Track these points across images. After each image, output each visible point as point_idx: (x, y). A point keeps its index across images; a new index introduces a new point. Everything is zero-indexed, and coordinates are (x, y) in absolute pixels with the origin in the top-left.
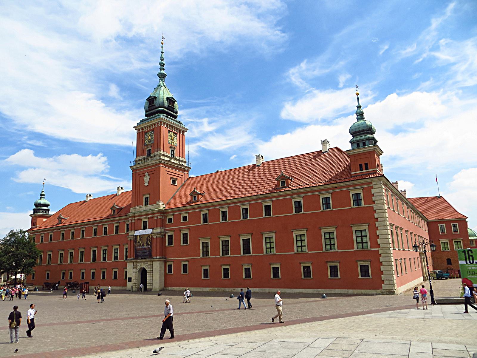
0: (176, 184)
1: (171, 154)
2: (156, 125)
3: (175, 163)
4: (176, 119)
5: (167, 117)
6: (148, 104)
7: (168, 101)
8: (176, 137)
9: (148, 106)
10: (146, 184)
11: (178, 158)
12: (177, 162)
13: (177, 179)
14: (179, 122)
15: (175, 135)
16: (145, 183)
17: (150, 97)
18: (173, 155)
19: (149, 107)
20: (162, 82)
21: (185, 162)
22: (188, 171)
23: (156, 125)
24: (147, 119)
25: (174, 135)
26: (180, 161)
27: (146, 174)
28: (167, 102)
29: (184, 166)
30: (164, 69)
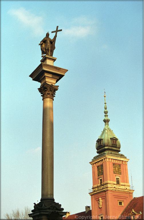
0: (123, 205)
1: (117, 181)
4: (119, 153)
5: (111, 153)
7: (111, 141)
11: (123, 184)
12: (123, 187)
13: (123, 201)
14: (122, 155)
17: (99, 139)
18: (118, 183)
20: (107, 125)
21: (129, 186)
24: (97, 156)
26: (124, 185)
28: (110, 142)
30: (107, 116)
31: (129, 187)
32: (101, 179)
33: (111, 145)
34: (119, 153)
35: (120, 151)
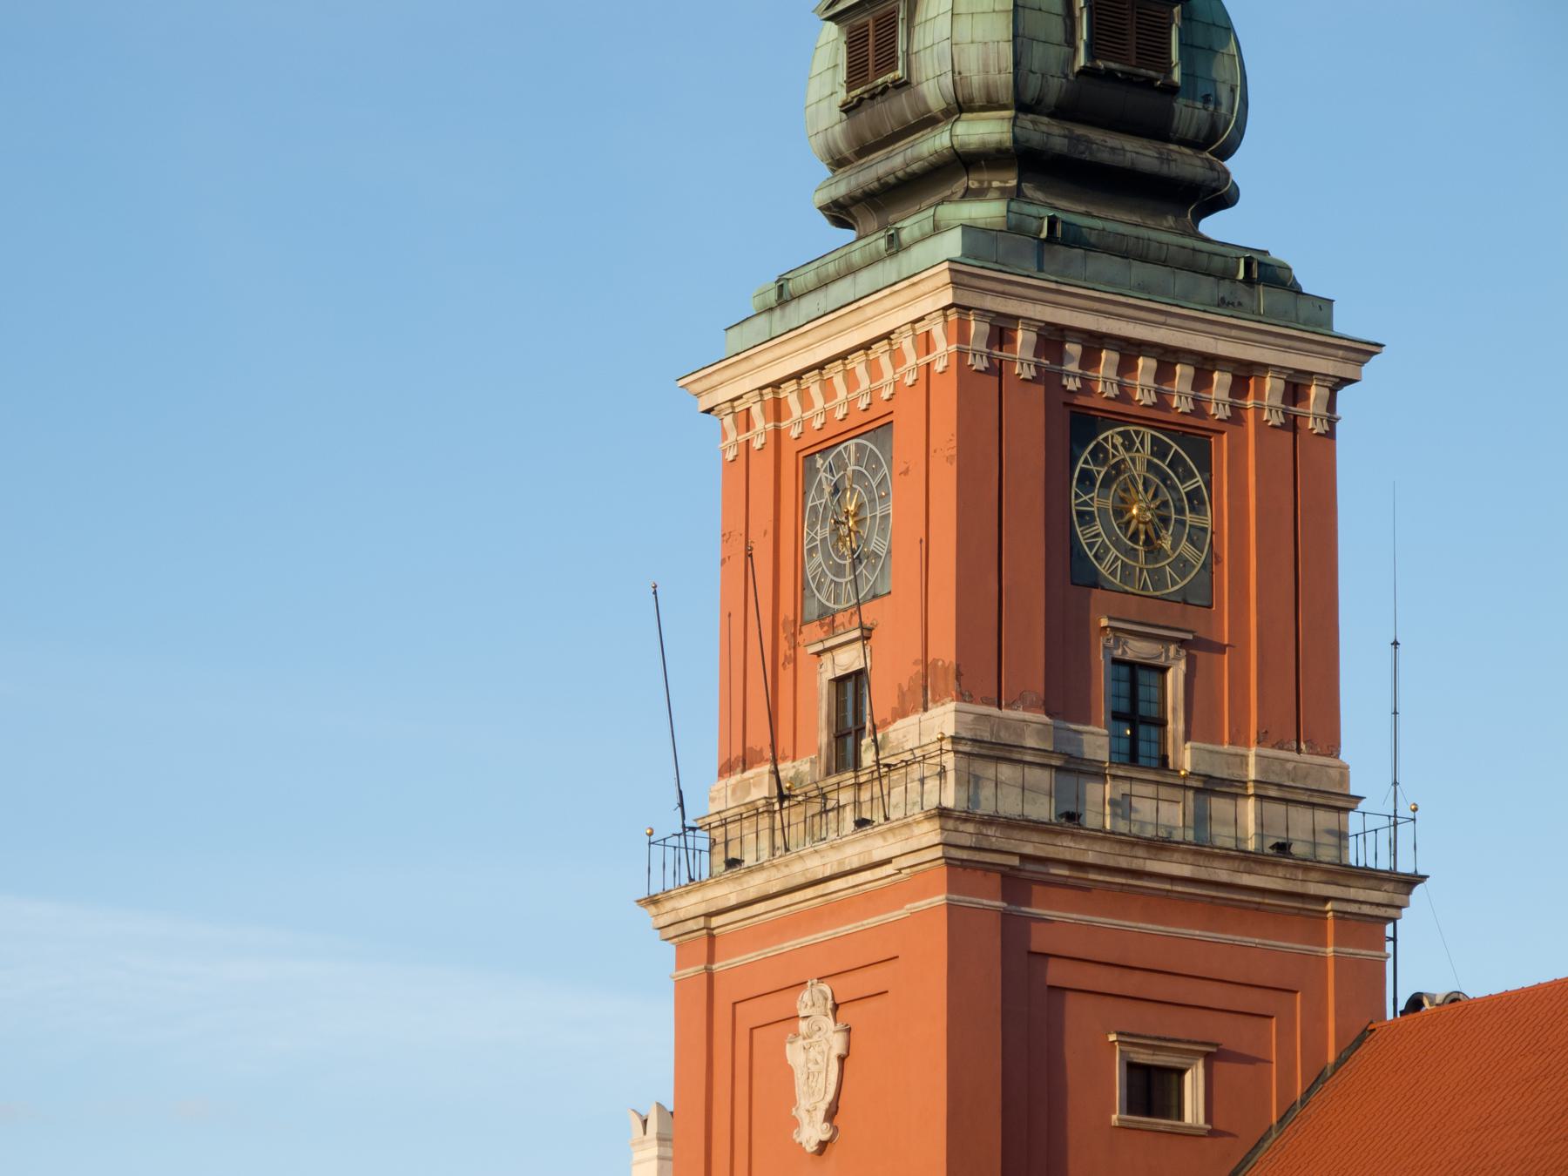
2: (911, 359)
3: (1161, 845)
6: (842, 75)
8: (1199, 480)
9: (842, 95)
10: (812, 1132)
15: (1175, 447)
16: (800, 1113)
19: (848, 109)
21: (1343, 803)
22: (1372, 927)
23: (911, 359)
25: (1160, 450)
27: (806, 996)
28: (1057, 30)
29: (1308, 865)
31: (1325, 819)
32: (849, 660)
33: (1056, 88)
34: (1215, 226)
35: (1220, 197)
